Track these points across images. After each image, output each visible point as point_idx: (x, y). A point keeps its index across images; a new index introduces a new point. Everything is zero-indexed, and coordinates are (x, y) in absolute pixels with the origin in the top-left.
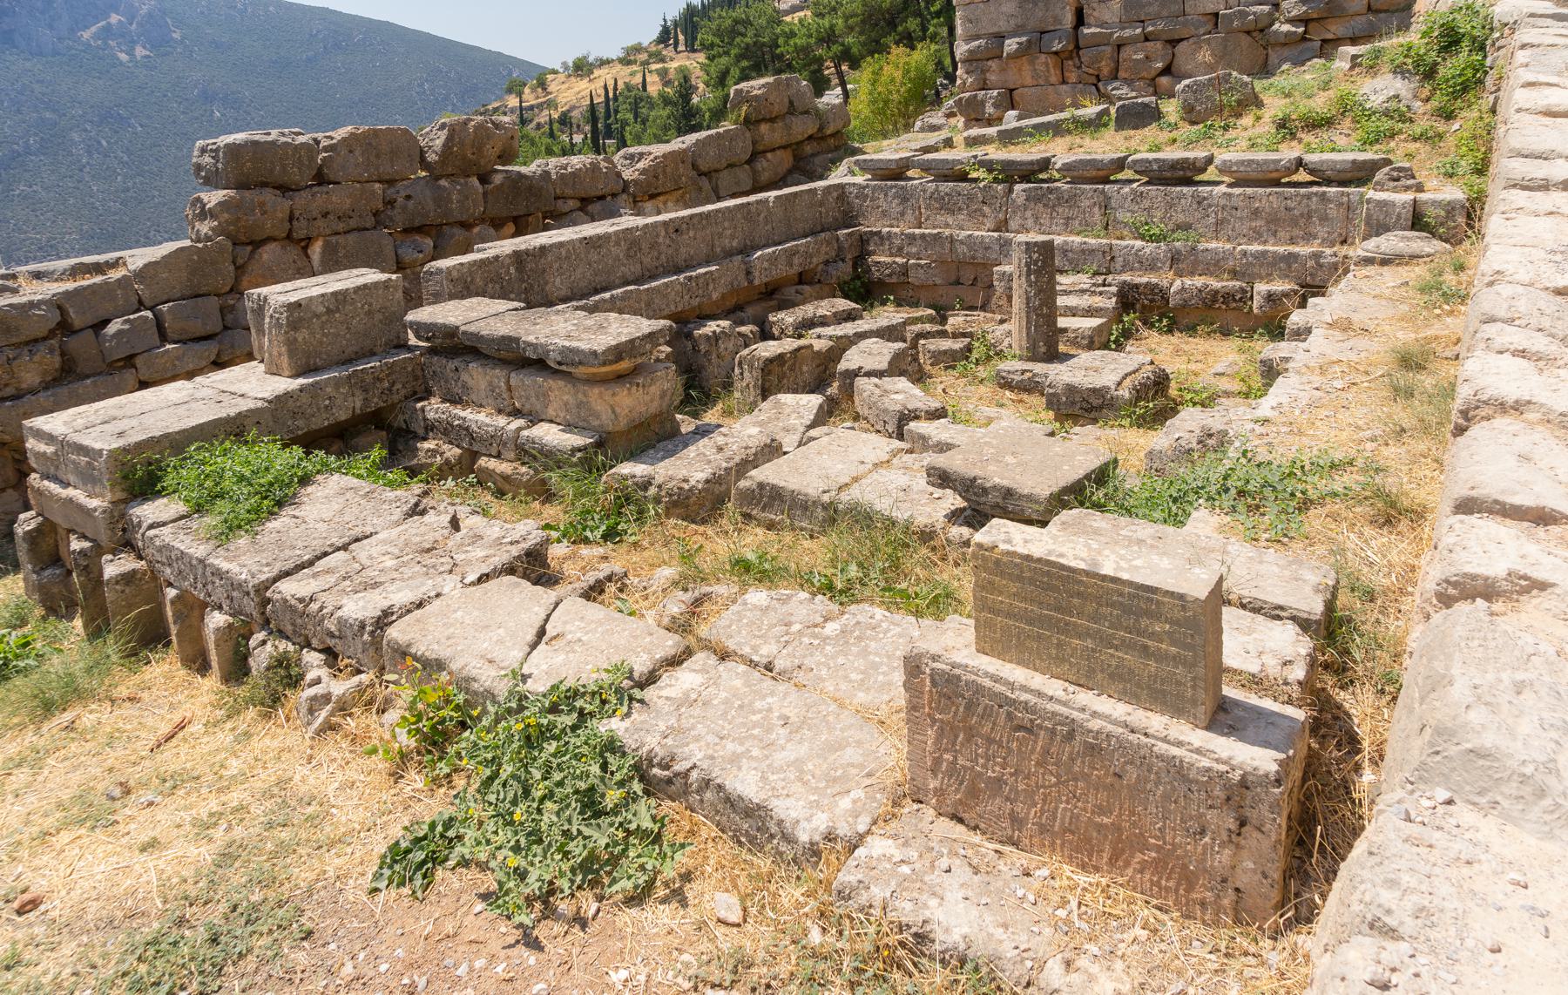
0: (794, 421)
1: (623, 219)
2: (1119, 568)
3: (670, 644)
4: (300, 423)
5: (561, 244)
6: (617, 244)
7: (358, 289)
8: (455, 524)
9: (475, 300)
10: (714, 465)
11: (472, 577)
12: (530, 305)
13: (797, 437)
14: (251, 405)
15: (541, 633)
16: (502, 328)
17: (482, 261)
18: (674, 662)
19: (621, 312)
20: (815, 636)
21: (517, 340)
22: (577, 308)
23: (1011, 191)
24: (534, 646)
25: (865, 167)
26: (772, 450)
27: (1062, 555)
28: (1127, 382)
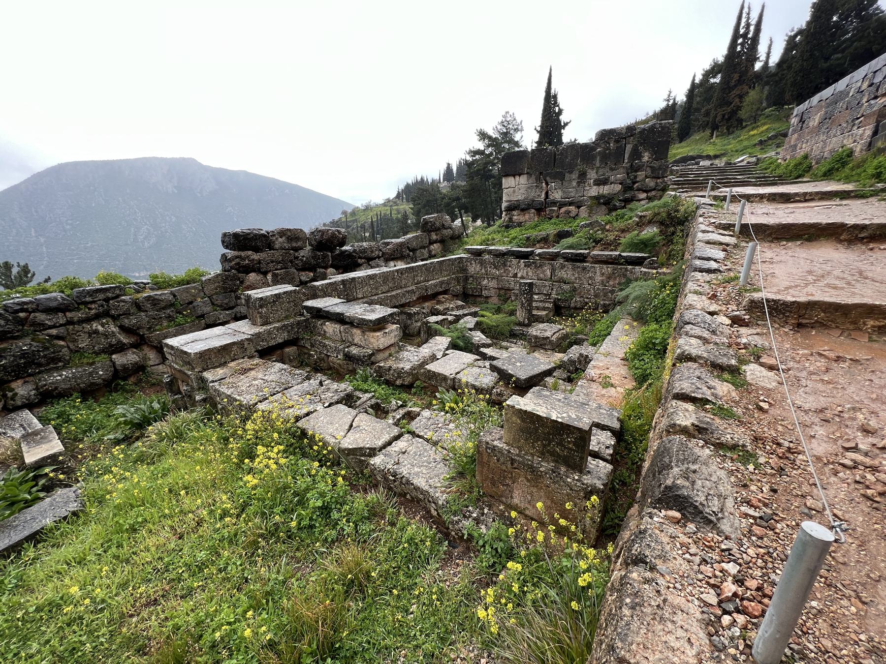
0: (440, 347)
1: (382, 268)
2: (557, 417)
3: (396, 431)
4: (265, 344)
5: (359, 278)
6: (380, 278)
7: (285, 293)
8: (321, 384)
9: (328, 298)
10: (413, 363)
11: (326, 405)
12: (348, 301)
13: (442, 353)
14: (246, 337)
15: (351, 426)
16: (338, 309)
17: (330, 283)
18: (397, 438)
19: (381, 305)
20: (446, 429)
21: (343, 314)
22: (364, 303)
23: (519, 262)
24: (349, 430)
25: (468, 251)
26: (433, 358)
27: (538, 411)
28: (555, 336)
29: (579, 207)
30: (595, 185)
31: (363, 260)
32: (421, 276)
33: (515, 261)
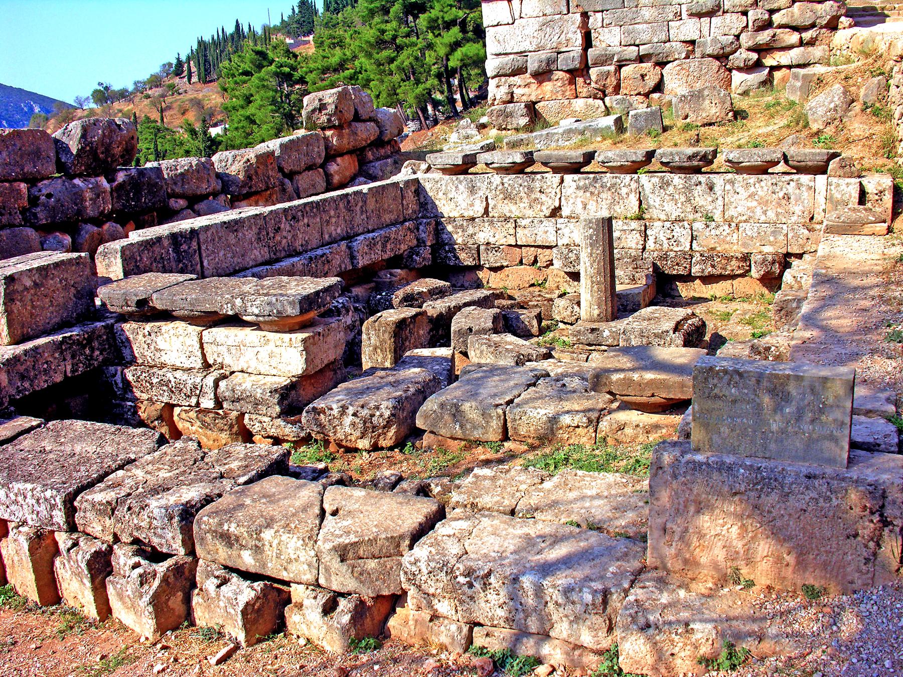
29: (662, 64)
30: (692, 15)
31: (182, 203)
32: (337, 225)
33: (553, 179)
